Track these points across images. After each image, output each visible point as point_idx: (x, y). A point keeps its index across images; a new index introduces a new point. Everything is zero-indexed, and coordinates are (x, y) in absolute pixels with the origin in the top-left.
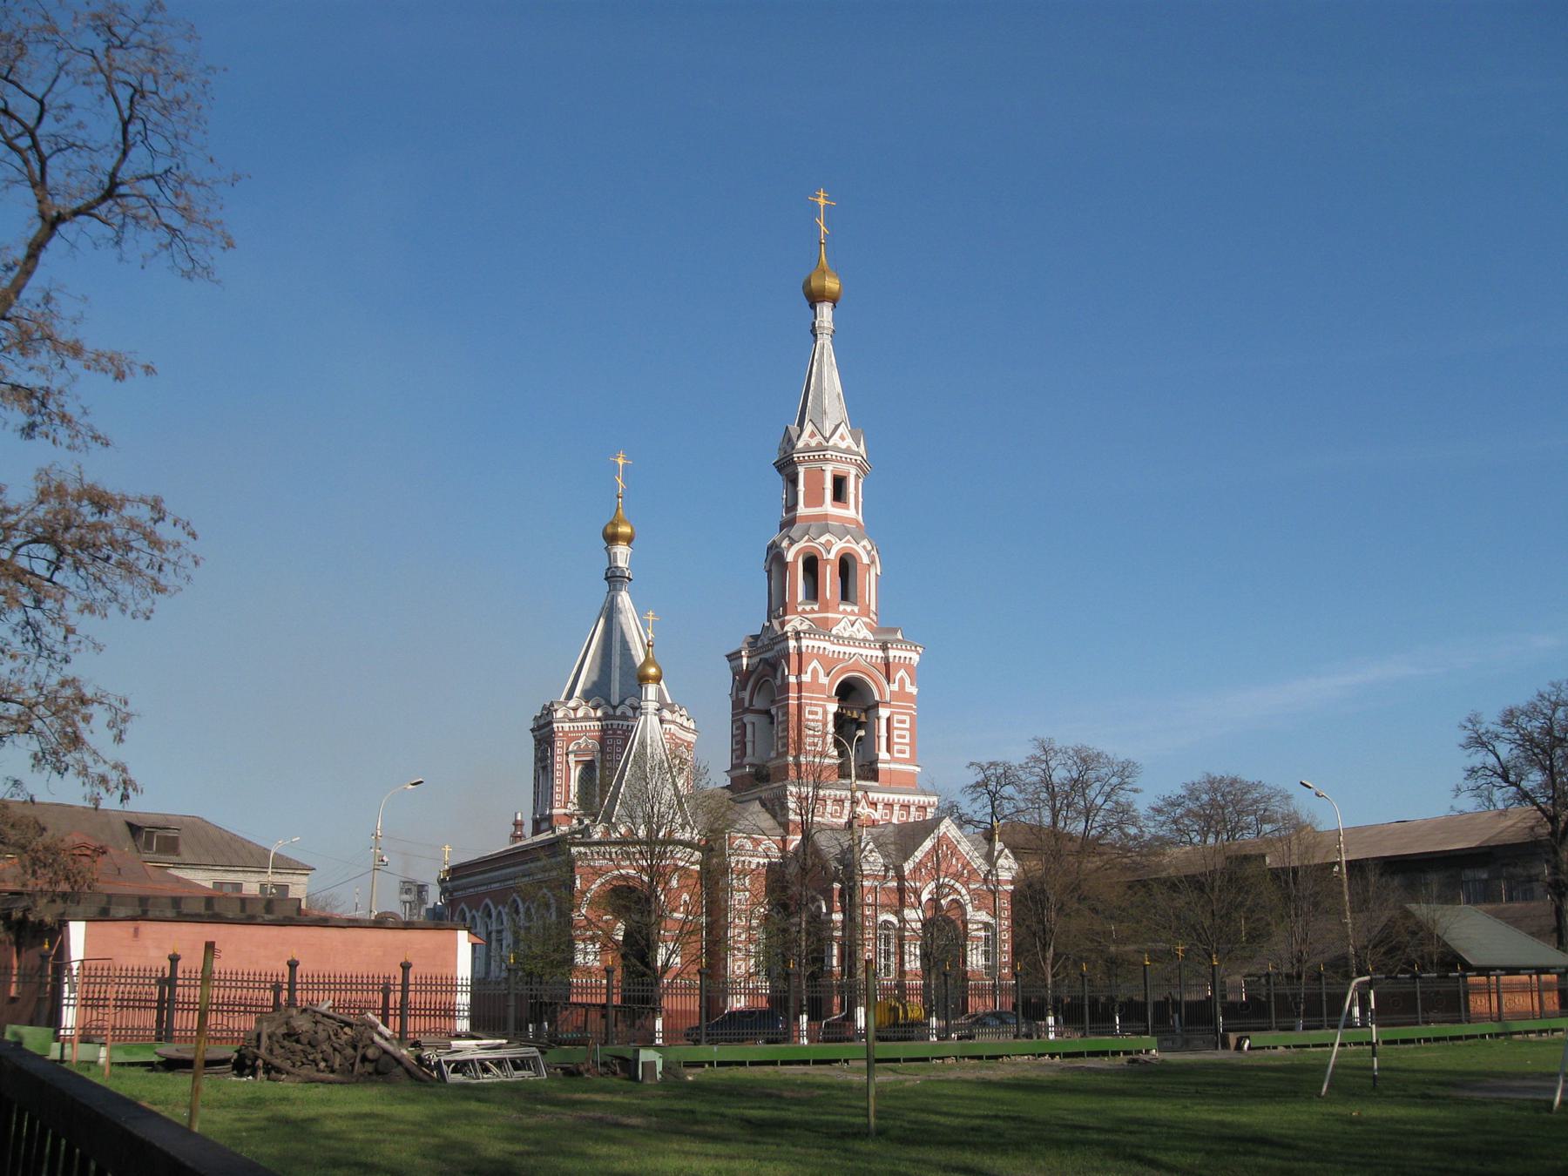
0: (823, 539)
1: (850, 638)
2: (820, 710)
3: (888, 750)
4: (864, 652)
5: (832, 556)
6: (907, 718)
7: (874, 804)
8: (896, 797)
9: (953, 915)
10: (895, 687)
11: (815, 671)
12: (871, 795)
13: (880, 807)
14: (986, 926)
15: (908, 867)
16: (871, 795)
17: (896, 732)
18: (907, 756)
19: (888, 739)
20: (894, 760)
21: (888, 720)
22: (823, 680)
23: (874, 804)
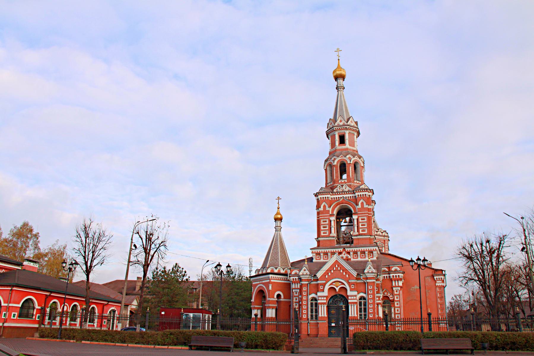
0: (333, 159)
1: (343, 191)
2: (327, 220)
3: (358, 231)
4: (347, 196)
5: (335, 163)
6: (366, 218)
7: (349, 253)
8: (358, 249)
9: (343, 293)
10: (360, 206)
11: (324, 206)
12: (346, 249)
13: (351, 253)
14: (362, 298)
15: (319, 275)
16: (346, 249)
17: (360, 224)
18: (366, 232)
19: (358, 227)
20: (360, 235)
21: (357, 219)
22: (327, 209)
23: (349, 253)
